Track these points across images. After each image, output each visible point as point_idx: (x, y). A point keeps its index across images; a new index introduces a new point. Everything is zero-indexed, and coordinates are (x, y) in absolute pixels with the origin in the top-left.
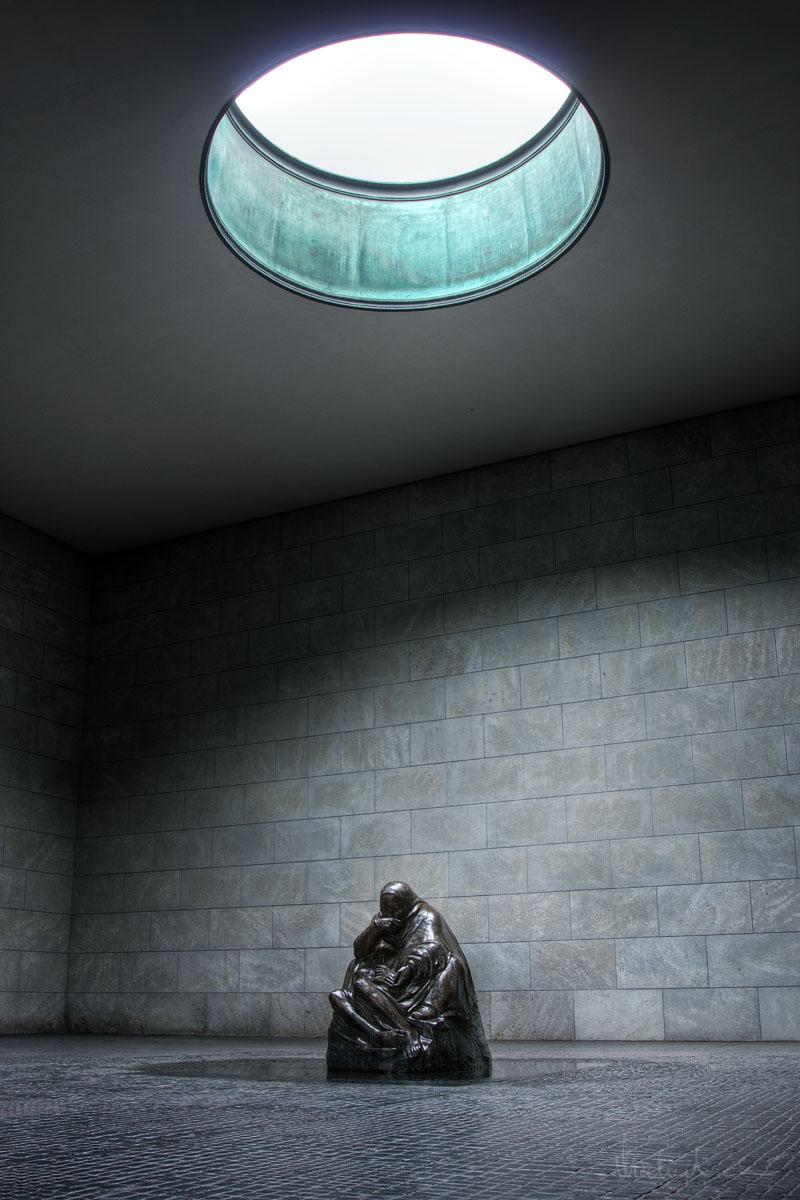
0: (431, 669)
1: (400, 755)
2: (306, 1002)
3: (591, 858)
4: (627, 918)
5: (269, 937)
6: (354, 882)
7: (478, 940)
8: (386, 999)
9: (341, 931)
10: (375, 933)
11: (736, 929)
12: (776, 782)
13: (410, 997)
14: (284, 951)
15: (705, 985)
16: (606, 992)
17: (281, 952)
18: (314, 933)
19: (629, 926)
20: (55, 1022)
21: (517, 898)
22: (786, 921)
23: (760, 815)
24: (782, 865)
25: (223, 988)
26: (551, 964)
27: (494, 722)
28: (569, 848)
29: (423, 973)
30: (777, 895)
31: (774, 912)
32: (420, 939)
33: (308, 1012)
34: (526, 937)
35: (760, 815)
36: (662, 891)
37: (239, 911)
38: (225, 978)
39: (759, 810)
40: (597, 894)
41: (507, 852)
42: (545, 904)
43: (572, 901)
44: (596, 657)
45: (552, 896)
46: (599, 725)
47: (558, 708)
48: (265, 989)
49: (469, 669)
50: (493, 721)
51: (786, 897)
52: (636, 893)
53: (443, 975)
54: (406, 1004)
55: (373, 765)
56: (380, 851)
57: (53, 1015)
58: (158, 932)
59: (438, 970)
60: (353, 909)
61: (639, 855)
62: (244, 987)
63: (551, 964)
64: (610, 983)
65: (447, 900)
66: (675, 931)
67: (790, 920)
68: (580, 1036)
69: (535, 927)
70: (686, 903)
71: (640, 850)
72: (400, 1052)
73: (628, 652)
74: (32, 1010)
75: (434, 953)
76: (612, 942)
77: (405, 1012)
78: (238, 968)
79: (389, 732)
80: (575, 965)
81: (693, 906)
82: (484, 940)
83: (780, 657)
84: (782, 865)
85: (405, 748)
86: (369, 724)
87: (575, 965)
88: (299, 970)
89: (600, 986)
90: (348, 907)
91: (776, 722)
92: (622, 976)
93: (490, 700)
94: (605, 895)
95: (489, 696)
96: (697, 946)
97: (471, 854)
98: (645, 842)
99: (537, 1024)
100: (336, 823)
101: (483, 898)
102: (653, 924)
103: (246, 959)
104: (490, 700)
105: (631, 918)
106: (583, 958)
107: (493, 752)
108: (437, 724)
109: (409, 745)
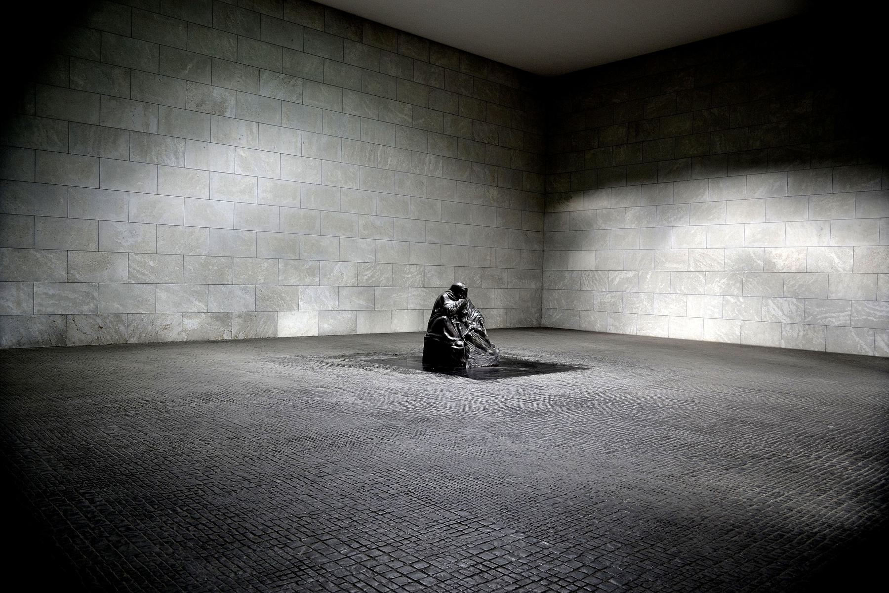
2: (99, 321)
3: (291, 243)
4: (305, 275)
5: (64, 273)
6: (139, 239)
7: (226, 283)
11: (351, 284)
12: (371, 218)
14: (79, 284)
15: (337, 309)
16: (293, 313)
17: (75, 285)
18: (106, 272)
22: (370, 282)
23: (364, 232)
24: (371, 256)
25: (16, 311)
26: (267, 297)
27: (242, 153)
28: (279, 236)
30: (367, 270)
31: (366, 277)
33: (101, 328)
34: (254, 283)
35: (364, 232)
37: (32, 251)
38: (19, 304)
39: (364, 230)
40: (292, 262)
41: (245, 233)
42: (266, 265)
44: (299, 132)
45: (269, 261)
46: (299, 170)
48: (60, 312)
51: (370, 271)
52: (310, 263)
56: (161, 221)
60: (138, 258)
61: (313, 244)
62: (39, 311)
63: (267, 297)
64: (295, 308)
65: (208, 257)
66: (326, 284)
67: (371, 281)
70: (332, 270)
71: (314, 242)
78: (33, 296)
79: (169, 140)
80: (279, 299)
81: (335, 272)
82: (230, 283)
83: (379, 159)
84: (371, 256)
87: (279, 299)
88: (93, 298)
89: (290, 309)
90: (134, 255)
91: (375, 190)
92: (301, 304)
94: (296, 263)
96: (334, 291)
97: (223, 231)
98: (316, 237)
99: (258, 330)
100: (126, 196)
101: (230, 258)
102: (317, 279)
103: (39, 289)
106: (283, 295)
107: (240, 172)
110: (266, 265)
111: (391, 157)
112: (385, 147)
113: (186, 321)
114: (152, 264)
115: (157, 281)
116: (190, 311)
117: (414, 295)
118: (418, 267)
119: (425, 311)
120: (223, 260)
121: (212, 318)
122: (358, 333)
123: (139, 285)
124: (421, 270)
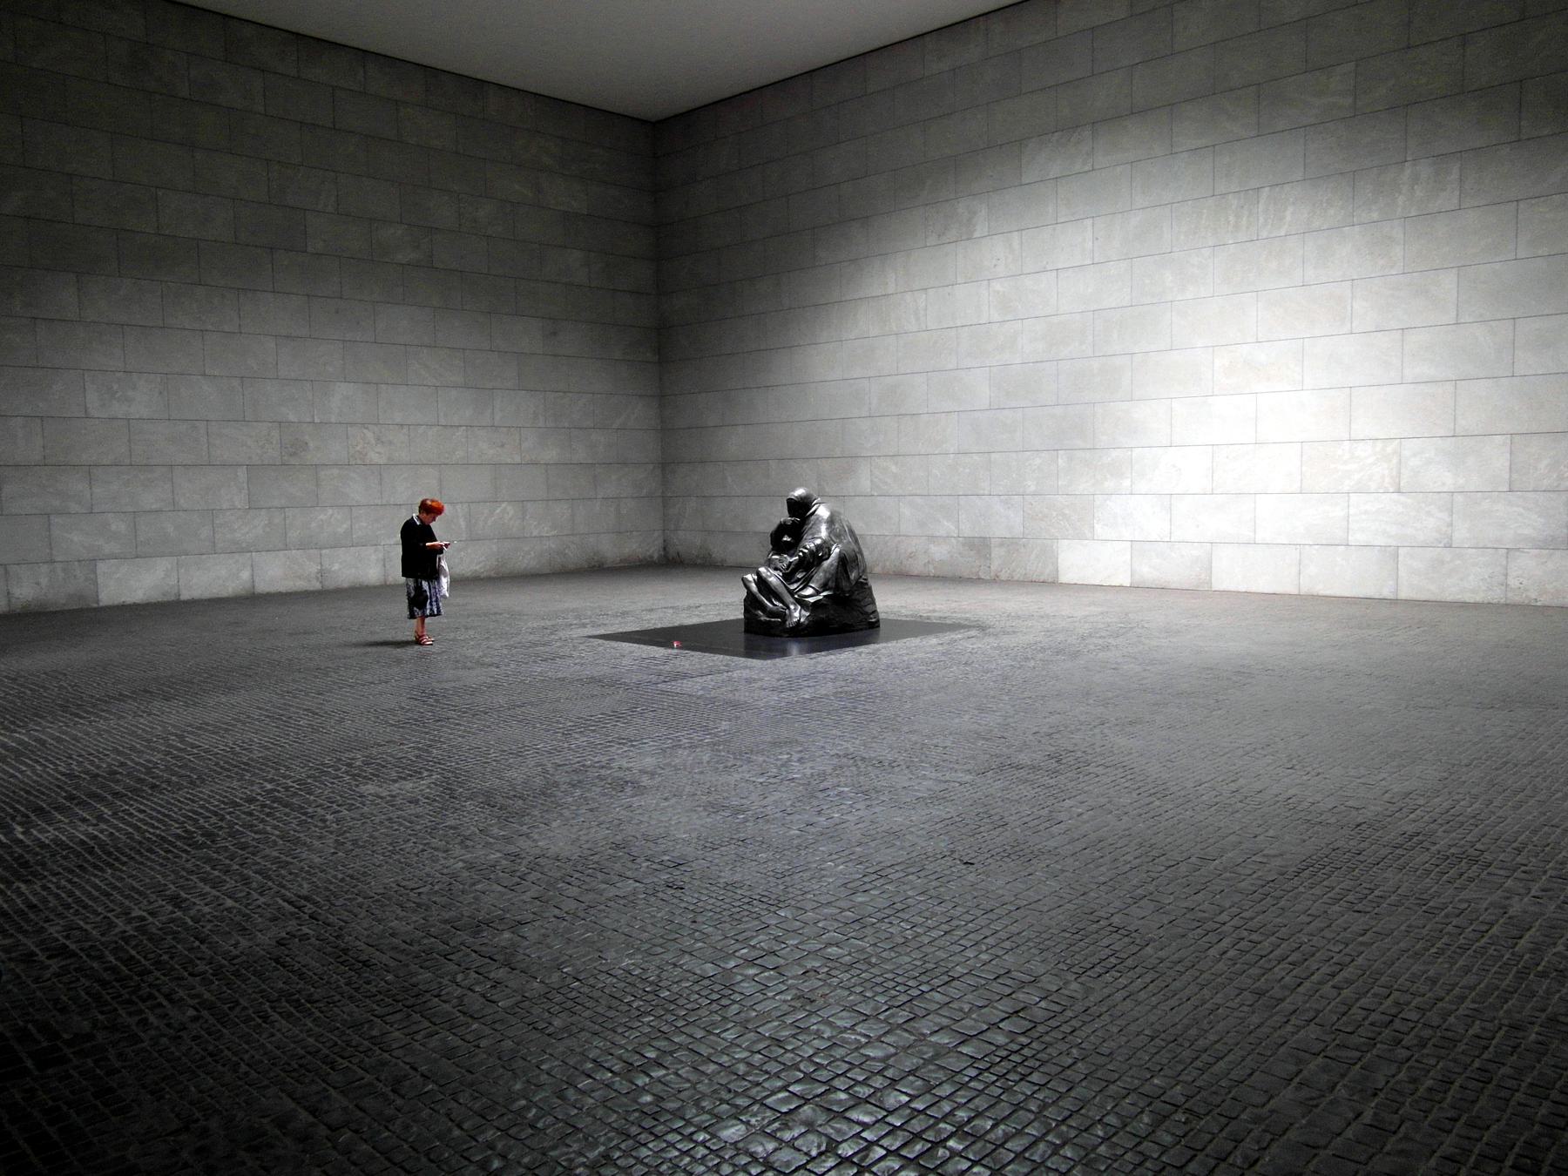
0: (944, 233)
1: (918, 319)
7: (982, 492)
8: (779, 582)
9: (872, 481)
10: (782, 529)
13: (799, 580)
19: (1107, 484)
20: (656, 556)
21: (1014, 455)
29: (812, 562)
32: (813, 534)
36: (1136, 451)
42: (1038, 461)
43: (1060, 461)
47: (1054, 273)
49: (976, 235)
50: (997, 286)
52: (1114, 454)
53: (826, 564)
54: (795, 586)
55: (895, 329)
57: (653, 549)
58: (729, 479)
59: (822, 559)
68: (1063, 579)
69: (1029, 483)
72: (784, 621)
73: (1120, 215)
74: (635, 547)
75: (819, 547)
76: (1091, 497)
77: (792, 593)
79: (908, 297)
82: (986, 492)
85: (922, 312)
86: (891, 289)
89: (1080, 537)
93: (995, 266)
95: (994, 262)
102: (1127, 483)
104: (995, 266)
105: (1108, 476)
106: (1067, 512)
108: (949, 289)
109: (926, 310)
110: (1038, 461)
111: (1293, 203)
112: (1277, 189)
113: (933, 548)
114: (894, 468)
115: (900, 492)
116: (938, 534)
117: (1366, 512)
118: (1379, 445)
119: (1401, 551)
120: (976, 457)
121: (964, 545)
122: (1217, 586)
123: (882, 498)
124: (1389, 449)
